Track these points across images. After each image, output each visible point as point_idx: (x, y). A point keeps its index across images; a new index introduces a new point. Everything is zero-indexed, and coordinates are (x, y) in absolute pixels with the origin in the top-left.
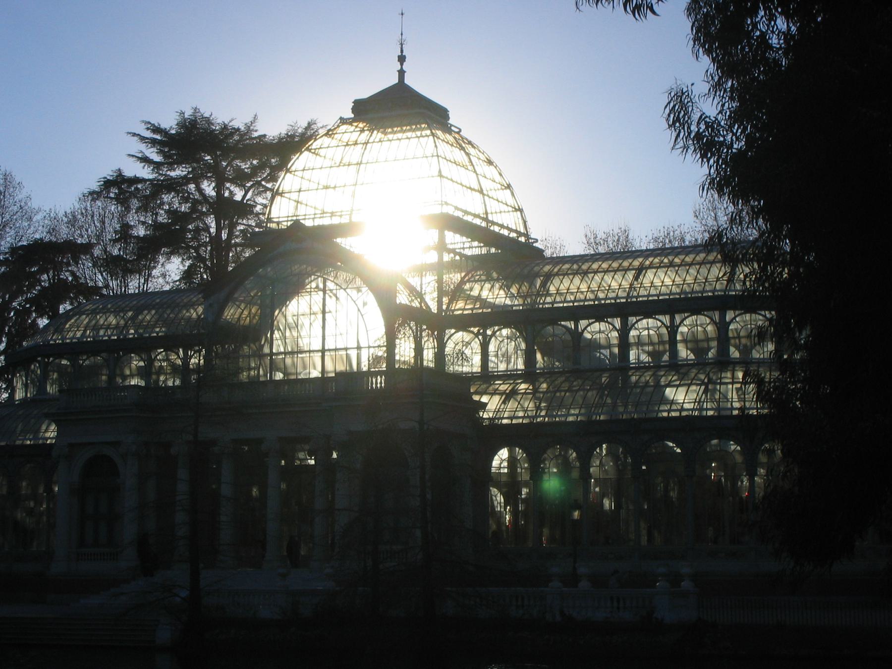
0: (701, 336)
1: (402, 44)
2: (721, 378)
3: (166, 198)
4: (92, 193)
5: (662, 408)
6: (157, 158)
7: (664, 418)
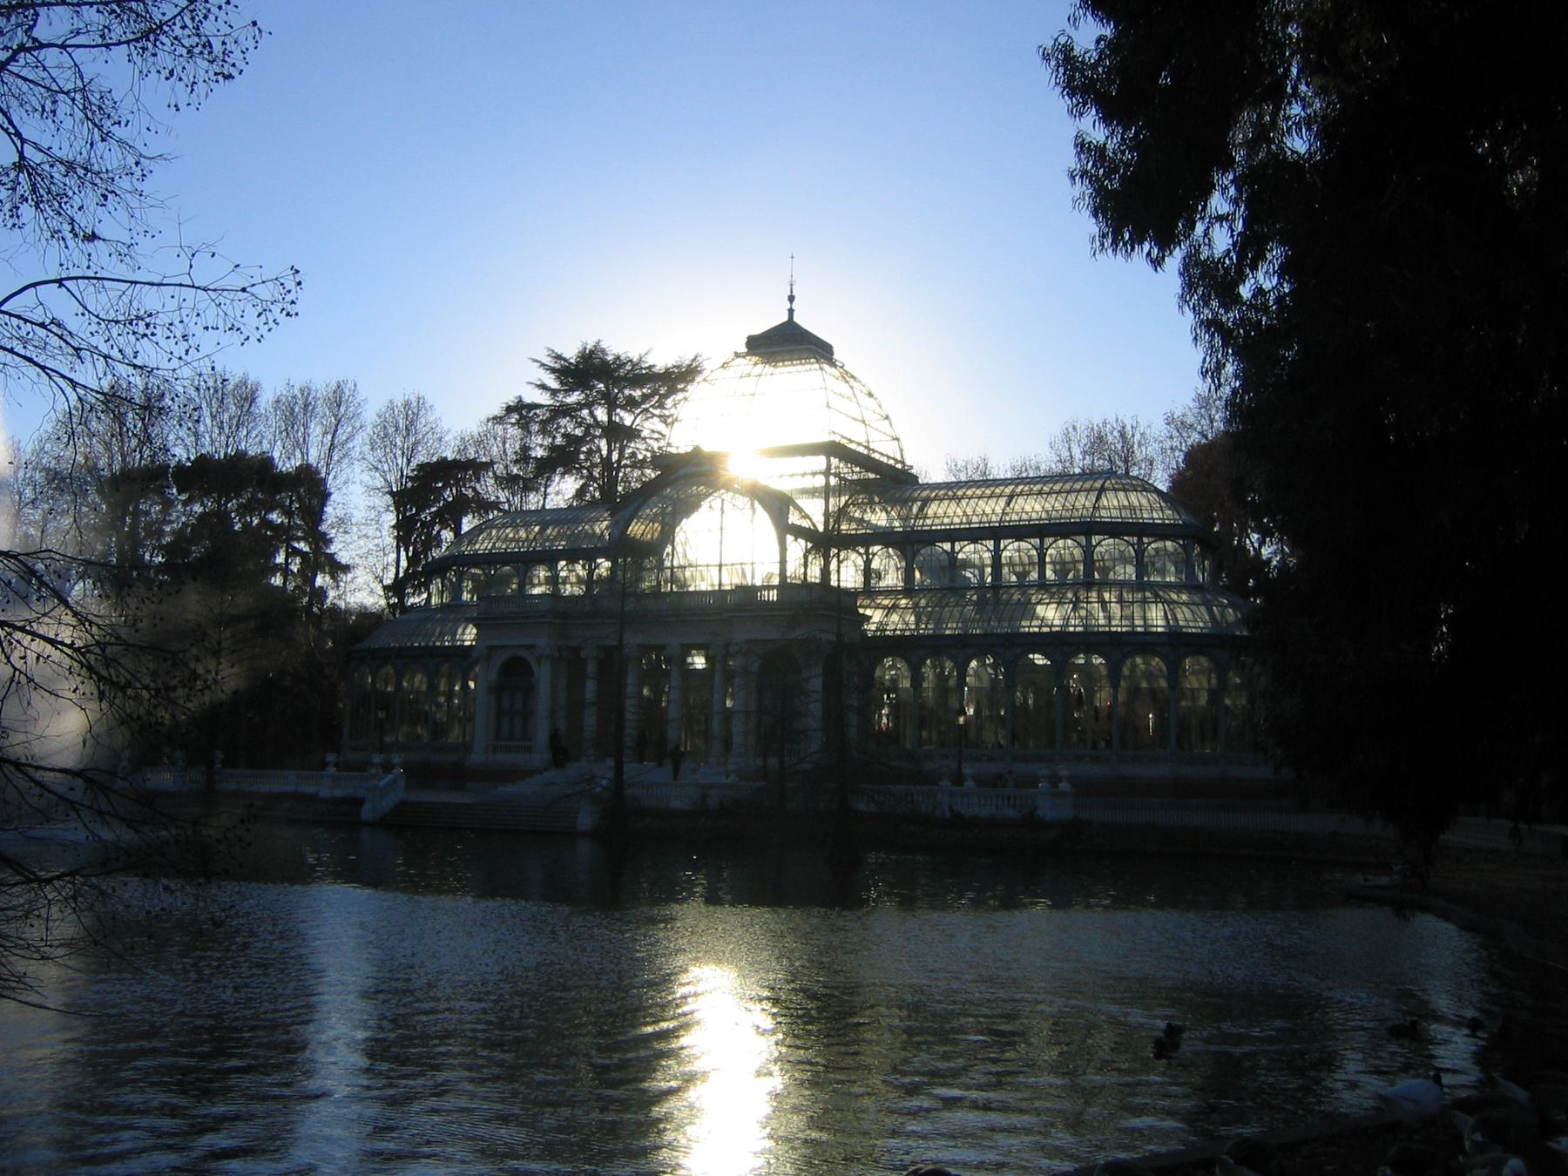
0: (1068, 558)
1: (791, 285)
2: (1087, 598)
3: (563, 422)
4: (495, 418)
5: (1023, 624)
6: (555, 385)
7: (1025, 633)
